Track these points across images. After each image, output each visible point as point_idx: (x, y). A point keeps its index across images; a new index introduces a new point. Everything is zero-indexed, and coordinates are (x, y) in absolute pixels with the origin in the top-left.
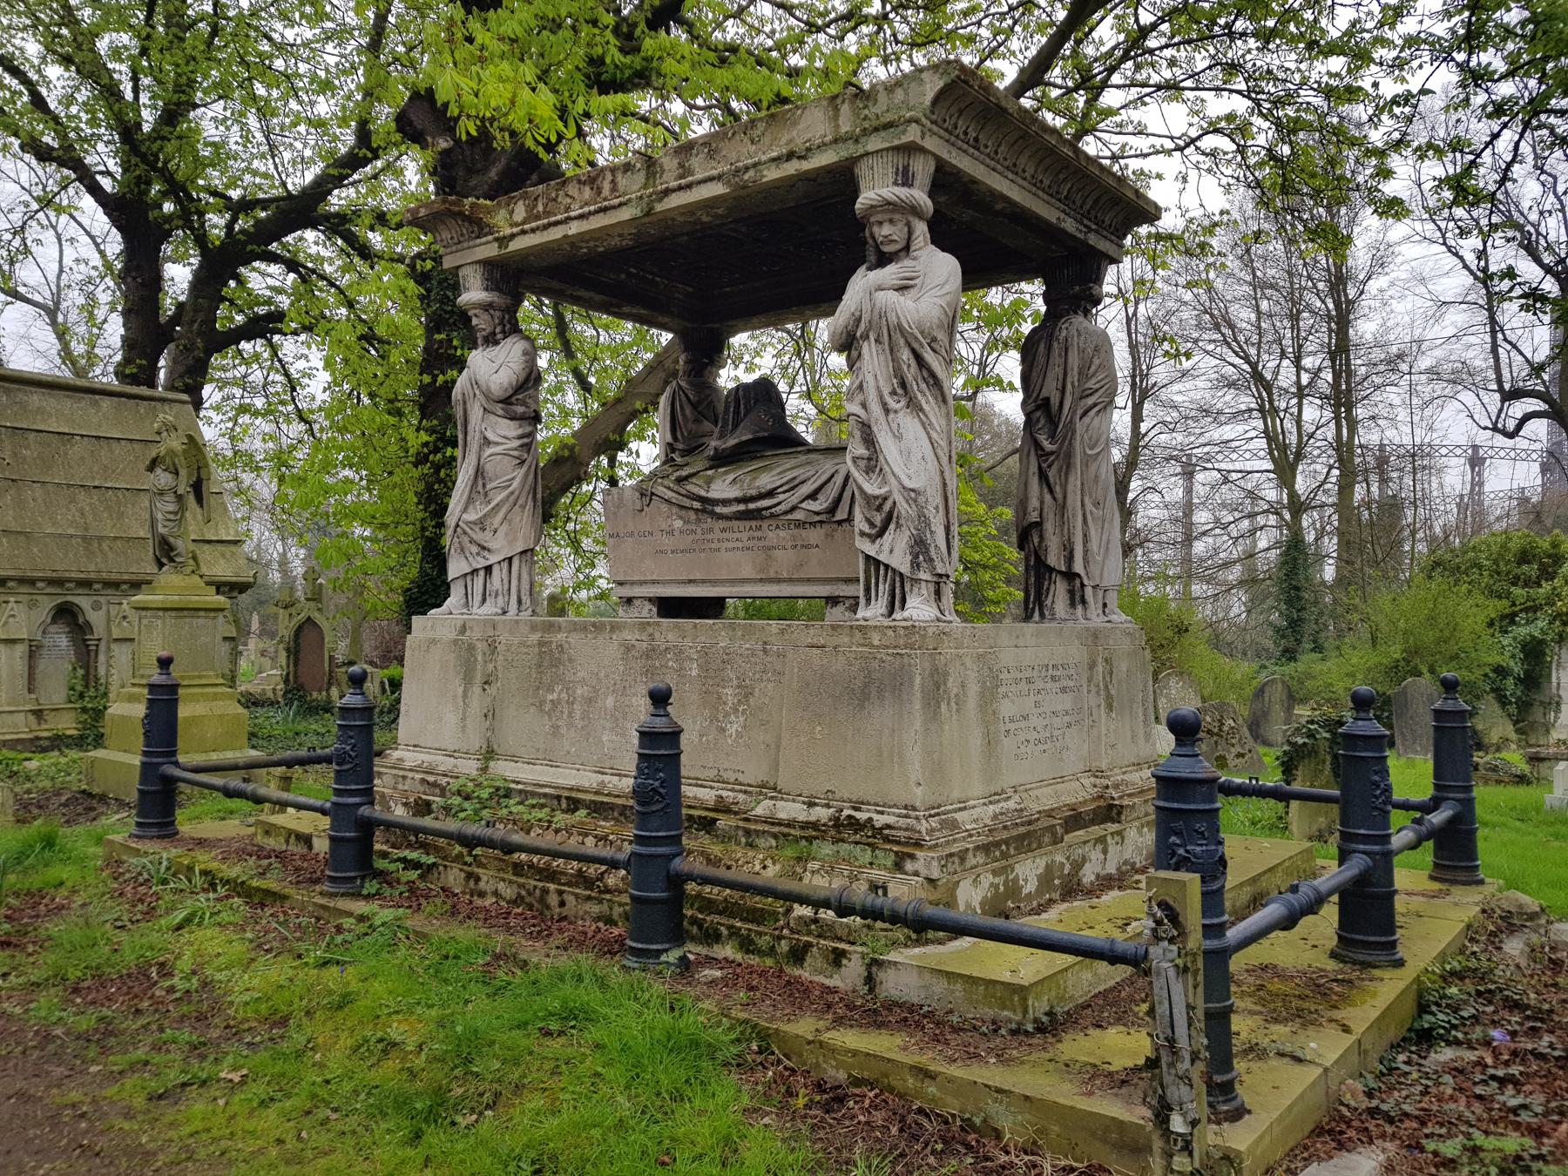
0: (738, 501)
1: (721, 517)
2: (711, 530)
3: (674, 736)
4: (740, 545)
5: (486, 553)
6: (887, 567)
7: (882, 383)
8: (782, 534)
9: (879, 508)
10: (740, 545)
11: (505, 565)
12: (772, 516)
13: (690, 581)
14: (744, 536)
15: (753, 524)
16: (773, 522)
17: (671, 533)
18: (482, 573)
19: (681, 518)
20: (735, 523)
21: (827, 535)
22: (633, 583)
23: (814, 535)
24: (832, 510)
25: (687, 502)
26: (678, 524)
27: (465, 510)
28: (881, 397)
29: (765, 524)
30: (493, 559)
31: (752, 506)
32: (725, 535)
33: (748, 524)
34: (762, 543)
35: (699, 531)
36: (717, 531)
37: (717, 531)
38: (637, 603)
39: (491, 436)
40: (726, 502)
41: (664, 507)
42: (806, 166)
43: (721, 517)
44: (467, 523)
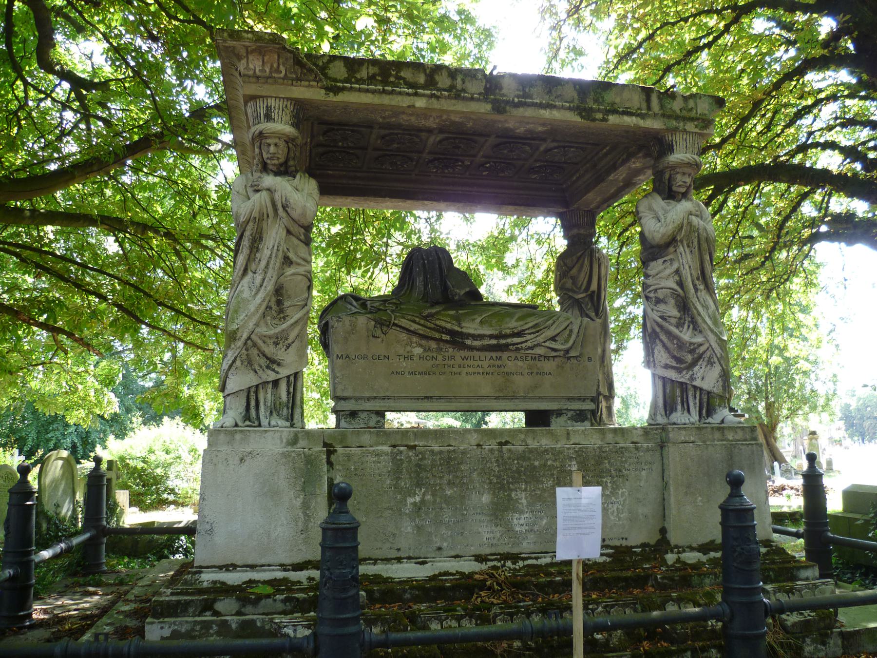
0: (491, 337)
1: (471, 348)
2: (452, 357)
3: (352, 531)
4: (481, 370)
5: (275, 366)
6: (701, 389)
7: (693, 272)
8: (520, 363)
9: (692, 352)
10: (481, 370)
11: (292, 379)
12: (518, 349)
13: (427, 398)
14: (485, 364)
15: (494, 355)
16: (513, 355)
17: (410, 357)
18: (270, 386)
19: (421, 346)
20: (483, 354)
21: (558, 367)
22: (357, 399)
23: (548, 366)
24: (567, 351)
25: (437, 335)
26: (418, 351)
27: (257, 325)
28: (693, 282)
29: (505, 355)
30: (284, 372)
31: (503, 341)
32: (466, 362)
33: (489, 354)
34: (502, 370)
35: (440, 357)
36: (458, 360)
37: (458, 360)
38: (363, 415)
39: (291, 255)
40: (475, 337)
41: (404, 336)
42: (642, 123)
43: (471, 348)
44: (263, 338)
